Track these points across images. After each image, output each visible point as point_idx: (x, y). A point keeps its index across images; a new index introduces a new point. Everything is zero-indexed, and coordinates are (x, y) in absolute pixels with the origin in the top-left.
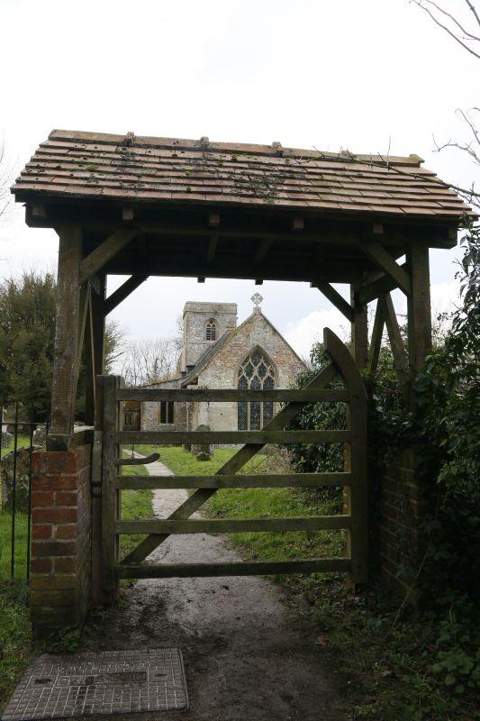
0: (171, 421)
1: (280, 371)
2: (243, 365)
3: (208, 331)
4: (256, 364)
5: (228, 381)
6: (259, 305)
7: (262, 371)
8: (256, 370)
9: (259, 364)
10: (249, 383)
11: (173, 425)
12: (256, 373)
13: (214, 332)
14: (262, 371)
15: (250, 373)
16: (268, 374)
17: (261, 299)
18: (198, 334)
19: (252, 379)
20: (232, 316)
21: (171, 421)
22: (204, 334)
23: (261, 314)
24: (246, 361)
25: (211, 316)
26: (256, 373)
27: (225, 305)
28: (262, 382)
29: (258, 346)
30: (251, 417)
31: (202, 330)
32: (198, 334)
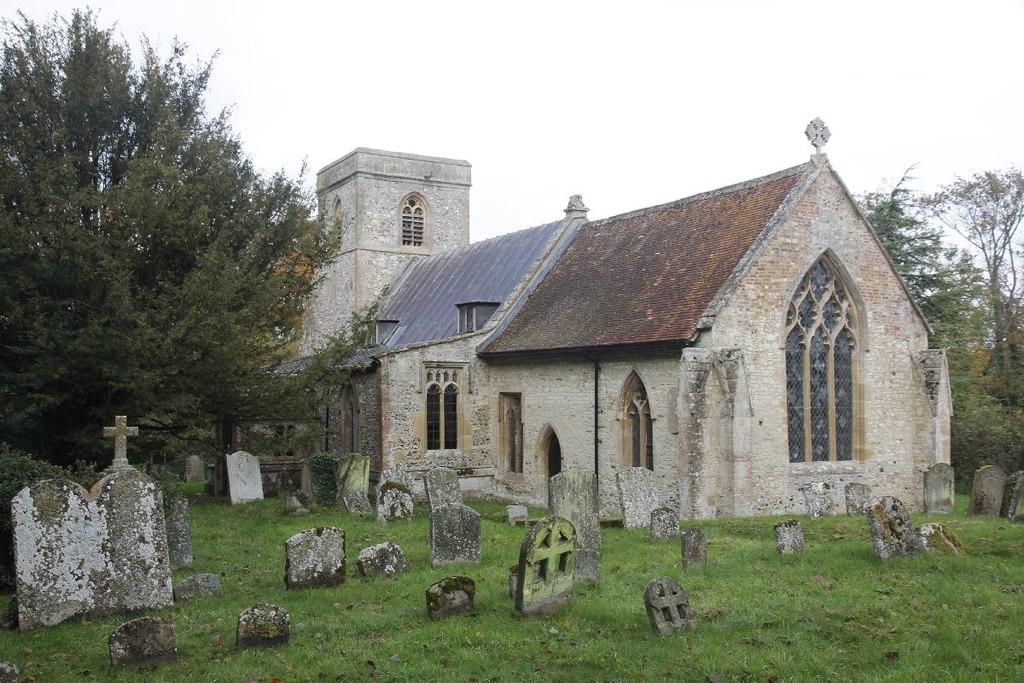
0: (451, 444)
1: (870, 314)
2: (796, 296)
3: (406, 224)
4: (819, 295)
5: (771, 337)
6: (824, 149)
7: (830, 318)
8: (820, 307)
9: (826, 297)
10: (807, 342)
11: (457, 452)
12: (819, 319)
13: (419, 228)
14: (830, 318)
15: (807, 317)
16: (842, 321)
17: (825, 139)
18: (384, 230)
19: (812, 332)
20: (461, 190)
21: (451, 444)
22: (397, 231)
23: (834, 174)
24: (802, 288)
25: (415, 187)
26: (819, 319)
27: (444, 161)
28: (832, 343)
29: (829, 249)
30: (813, 428)
31: (394, 215)
32: (384, 230)
